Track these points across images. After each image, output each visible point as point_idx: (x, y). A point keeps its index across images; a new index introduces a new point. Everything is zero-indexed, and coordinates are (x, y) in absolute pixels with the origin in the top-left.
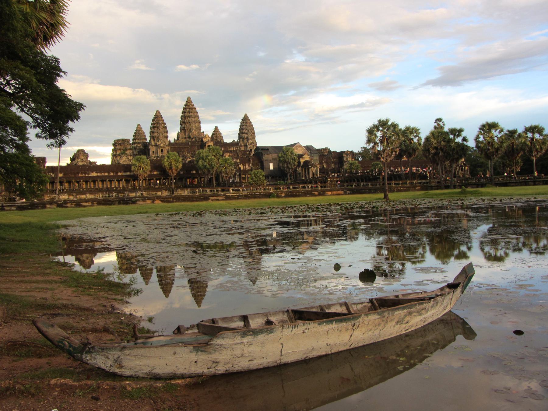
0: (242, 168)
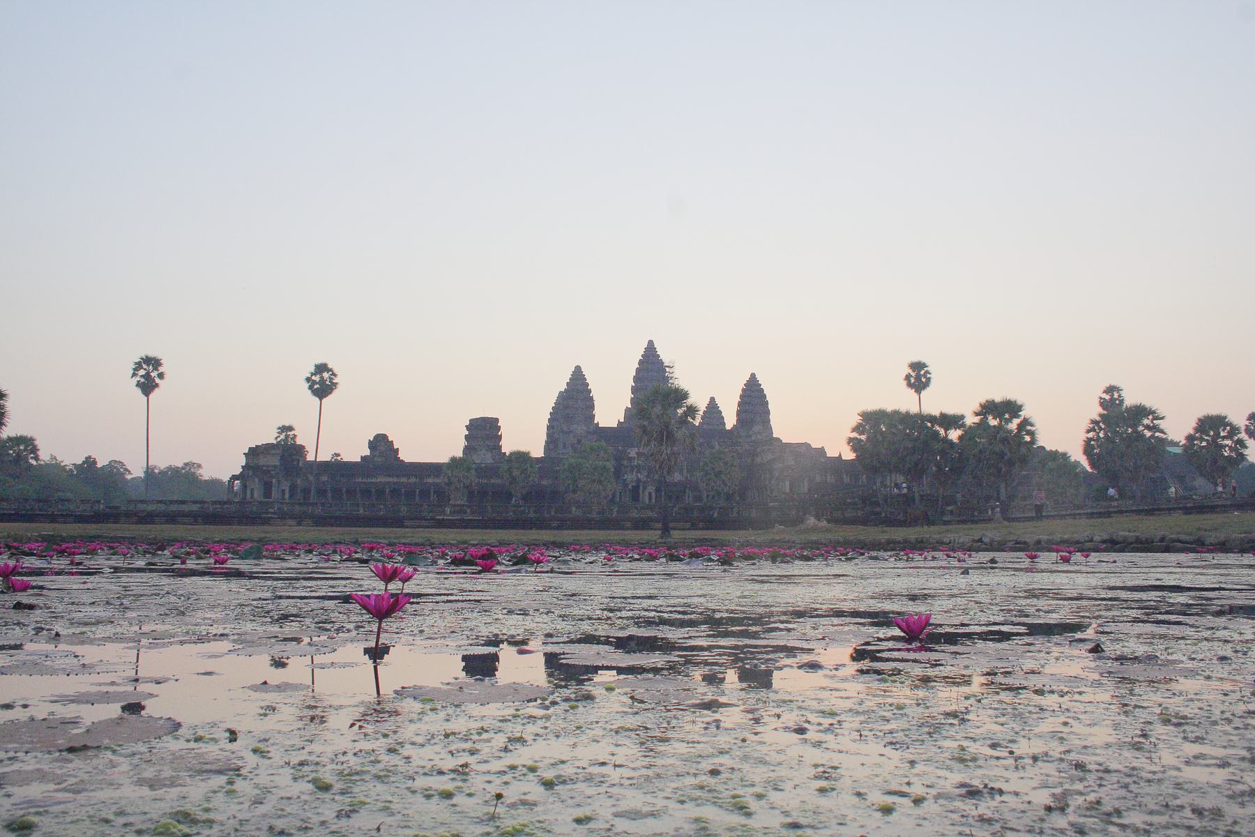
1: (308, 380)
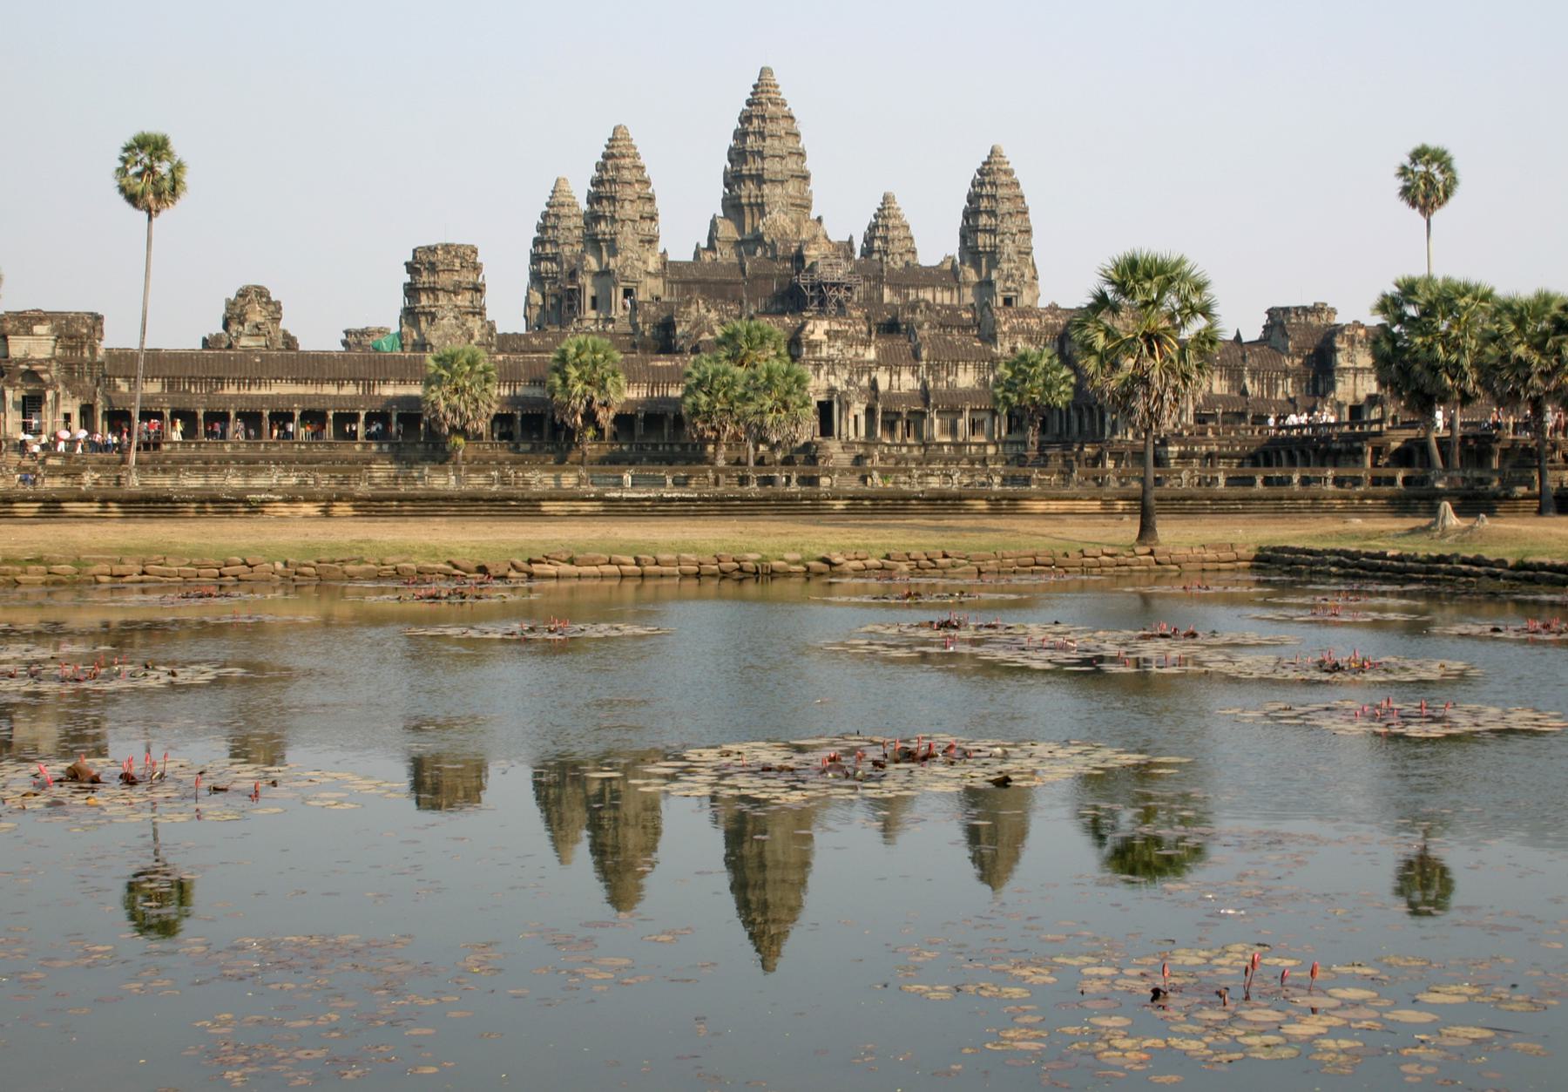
0: (883, 386)
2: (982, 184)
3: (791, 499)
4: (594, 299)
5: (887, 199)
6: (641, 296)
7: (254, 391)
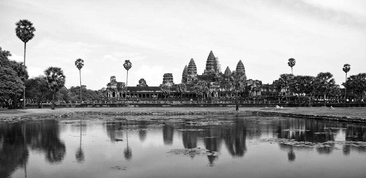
0: (220, 90)
1: (124, 65)
2: (238, 65)
3: (195, 104)
4: (189, 80)
5: (228, 67)
6: (194, 79)
7: (141, 92)
